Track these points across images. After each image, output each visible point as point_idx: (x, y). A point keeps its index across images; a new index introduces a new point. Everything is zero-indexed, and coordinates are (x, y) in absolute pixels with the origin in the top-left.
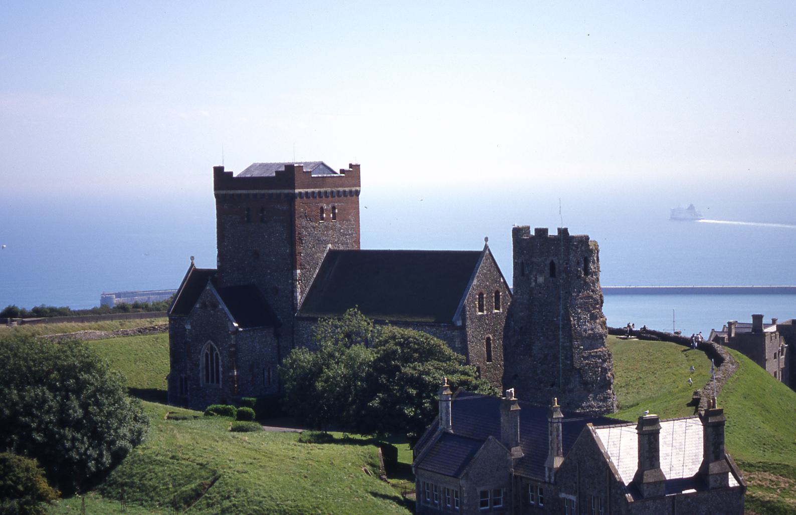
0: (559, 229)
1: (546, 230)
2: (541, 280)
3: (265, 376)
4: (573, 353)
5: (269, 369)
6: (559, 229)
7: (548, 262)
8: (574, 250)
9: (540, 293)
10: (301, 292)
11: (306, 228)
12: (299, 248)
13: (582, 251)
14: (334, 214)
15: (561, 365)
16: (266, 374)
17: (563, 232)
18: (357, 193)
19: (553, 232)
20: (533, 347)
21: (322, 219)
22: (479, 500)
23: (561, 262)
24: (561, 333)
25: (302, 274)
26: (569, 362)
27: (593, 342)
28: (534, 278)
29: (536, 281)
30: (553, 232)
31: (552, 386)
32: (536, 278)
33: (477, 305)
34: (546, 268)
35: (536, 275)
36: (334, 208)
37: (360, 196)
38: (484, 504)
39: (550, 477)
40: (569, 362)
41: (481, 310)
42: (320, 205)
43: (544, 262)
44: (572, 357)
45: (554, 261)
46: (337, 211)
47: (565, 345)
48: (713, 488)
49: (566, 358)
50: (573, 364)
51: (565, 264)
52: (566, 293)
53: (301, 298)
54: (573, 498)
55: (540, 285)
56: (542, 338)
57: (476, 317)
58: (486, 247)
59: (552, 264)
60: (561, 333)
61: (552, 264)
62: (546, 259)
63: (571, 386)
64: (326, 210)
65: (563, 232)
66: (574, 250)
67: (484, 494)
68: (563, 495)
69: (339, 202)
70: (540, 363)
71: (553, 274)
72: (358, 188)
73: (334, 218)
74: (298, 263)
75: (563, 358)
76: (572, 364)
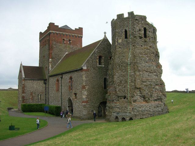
0: (129, 13)
1: (123, 14)
2: (120, 41)
4: (135, 78)
6: (129, 13)
7: (124, 30)
9: (120, 48)
13: (142, 24)
15: (129, 86)
16: (39, 96)
17: (131, 14)
18: (82, 37)
21: (64, 43)
23: (130, 30)
24: (129, 67)
25: (52, 61)
26: (133, 84)
27: (150, 74)
31: (124, 98)
32: (118, 40)
34: (123, 34)
36: (70, 40)
40: (133, 84)
41: (100, 64)
42: (64, 38)
44: (135, 80)
46: (71, 41)
49: (132, 82)
52: (133, 46)
58: (105, 36)
59: (126, 31)
60: (129, 67)
61: (126, 31)
62: (122, 30)
63: (135, 99)
64: (66, 40)
65: (131, 14)
71: (126, 37)
73: (70, 43)
75: (130, 82)
76: (135, 85)
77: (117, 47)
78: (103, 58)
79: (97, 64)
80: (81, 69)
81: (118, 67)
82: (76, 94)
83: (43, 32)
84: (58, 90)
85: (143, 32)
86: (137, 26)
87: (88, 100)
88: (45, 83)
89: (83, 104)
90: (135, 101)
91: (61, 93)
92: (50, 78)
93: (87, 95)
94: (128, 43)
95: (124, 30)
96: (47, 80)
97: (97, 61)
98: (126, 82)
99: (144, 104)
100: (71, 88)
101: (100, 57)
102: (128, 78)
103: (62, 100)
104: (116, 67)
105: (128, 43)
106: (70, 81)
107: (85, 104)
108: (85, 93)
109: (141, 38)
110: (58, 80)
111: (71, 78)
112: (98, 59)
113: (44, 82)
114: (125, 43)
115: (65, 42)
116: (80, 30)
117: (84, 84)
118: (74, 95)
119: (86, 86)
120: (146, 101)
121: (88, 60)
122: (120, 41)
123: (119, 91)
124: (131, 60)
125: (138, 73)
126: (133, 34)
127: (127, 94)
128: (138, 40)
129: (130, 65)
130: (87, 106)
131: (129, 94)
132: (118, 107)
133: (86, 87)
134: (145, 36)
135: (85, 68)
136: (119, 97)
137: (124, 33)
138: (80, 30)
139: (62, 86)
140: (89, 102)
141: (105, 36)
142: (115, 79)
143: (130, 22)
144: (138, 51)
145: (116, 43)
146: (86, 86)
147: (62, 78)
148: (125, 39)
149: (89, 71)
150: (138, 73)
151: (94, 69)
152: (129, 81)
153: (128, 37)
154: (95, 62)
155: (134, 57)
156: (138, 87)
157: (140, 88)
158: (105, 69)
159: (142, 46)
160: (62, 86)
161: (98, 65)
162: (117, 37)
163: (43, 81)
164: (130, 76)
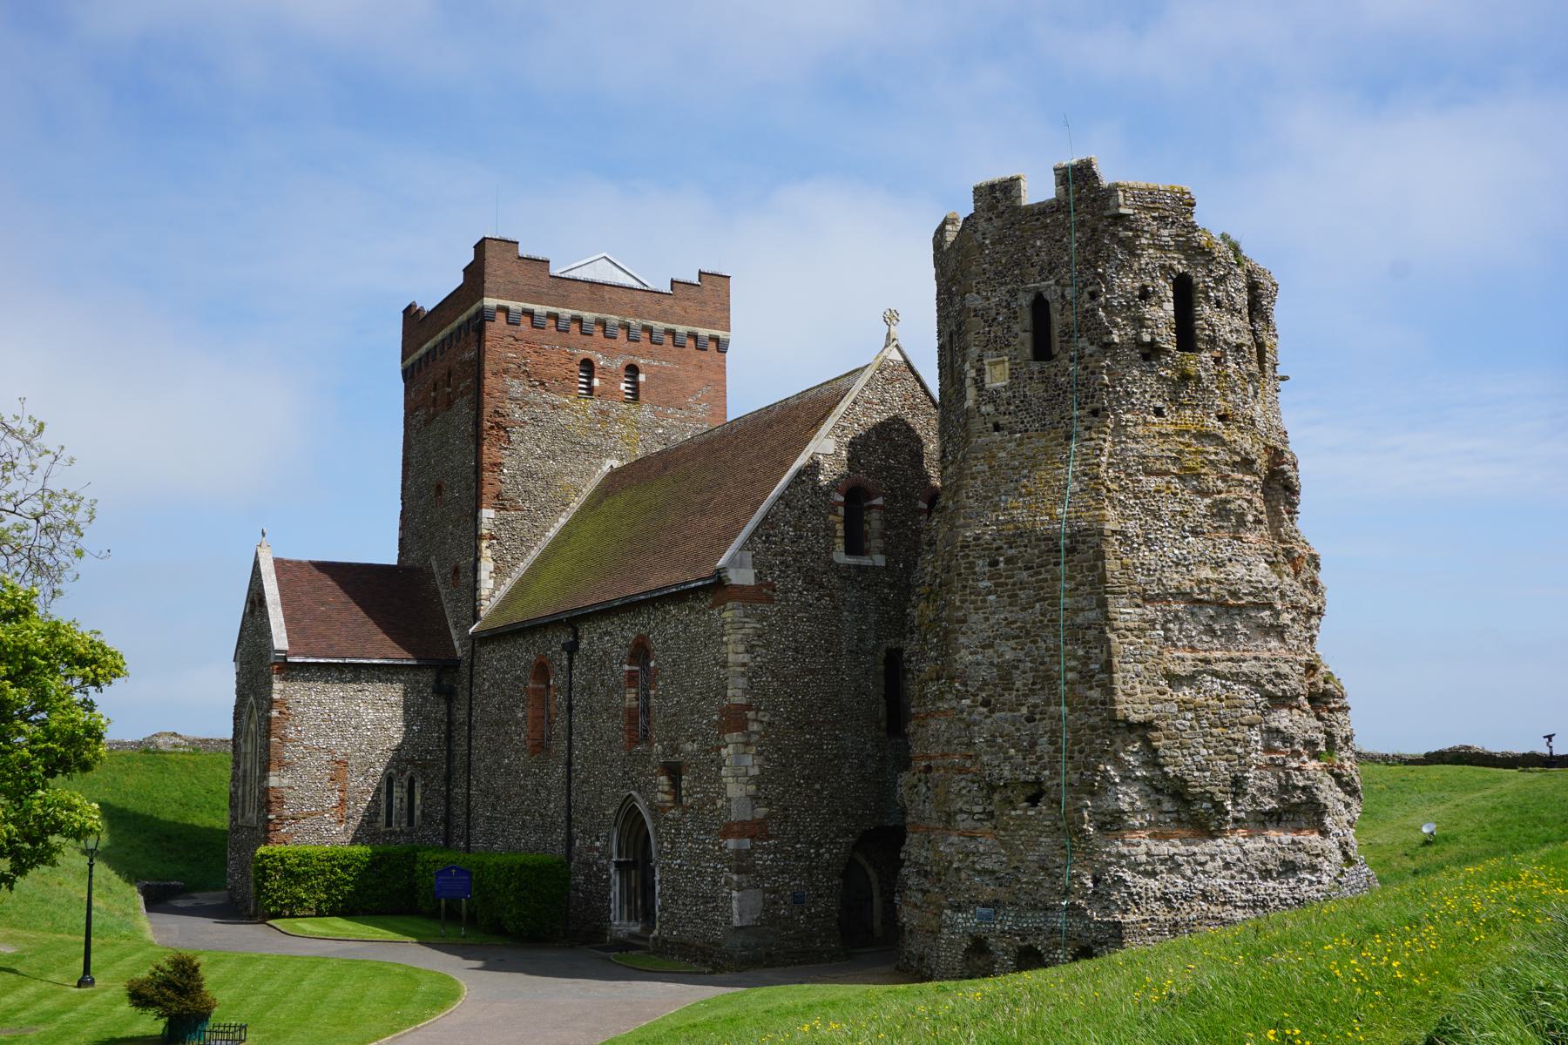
2: (997, 378)
3: (396, 802)
5: (412, 781)
7: (1025, 300)
8: (1122, 242)
9: (997, 427)
10: (497, 570)
11: (523, 403)
12: (490, 453)
14: (636, 383)
15: (1064, 709)
18: (721, 346)
20: (962, 639)
23: (1070, 293)
28: (973, 373)
29: (979, 383)
31: (1033, 800)
32: (980, 371)
33: (840, 527)
34: (1016, 328)
35: (980, 359)
40: (1095, 694)
41: (855, 545)
42: (583, 354)
43: (1008, 306)
44: (1108, 667)
45: (1047, 296)
46: (642, 378)
47: (1079, 620)
49: (1086, 677)
50: (1113, 702)
51: (1086, 296)
52: (1095, 413)
53: (496, 588)
55: (993, 398)
56: (992, 597)
57: (837, 568)
59: (1040, 306)
61: (1040, 306)
62: (1013, 293)
66: (1122, 242)
69: (652, 355)
70: (986, 703)
71: (1042, 351)
72: (720, 334)
74: (488, 491)
75: (1070, 675)
77: (977, 424)
78: (879, 501)
79: (829, 550)
80: (717, 587)
81: (981, 566)
82: (674, 771)
84: (540, 747)
85: (1169, 307)
86: (1121, 267)
87: (769, 816)
89: (731, 844)
91: (569, 764)
92: (485, 652)
93: (758, 781)
94: (1056, 396)
95: (1030, 297)
96: (464, 669)
97: (830, 529)
98: (1046, 680)
100: (638, 724)
102: (1058, 648)
103: (569, 818)
104: (972, 565)
106: (632, 677)
107: (747, 844)
108: (748, 760)
109: (1151, 352)
110: (542, 671)
111: (640, 651)
112: (841, 510)
113: (438, 681)
114: (1035, 390)
115: (596, 382)
117: (736, 695)
118: (663, 779)
119: (749, 707)
121: (765, 519)
123: (991, 742)
125: (1125, 613)
127: (1053, 765)
129: (1071, 551)
130: (763, 860)
131: (1063, 767)
132: (989, 864)
133: (751, 715)
135: (743, 576)
136: (993, 789)
137: (1026, 319)
139: (570, 708)
140: (773, 828)
142: (965, 656)
143: (1074, 239)
145: (971, 393)
146: (749, 707)
147: (572, 648)
148: (1035, 366)
149: (770, 600)
151: (811, 581)
153: (1056, 347)
154: (815, 531)
156: (1134, 718)
157: (1148, 725)
158: (891, 586)
159: (1158, 412)
160: (570, 708)
161: (840, 557)
162: (974, 351)
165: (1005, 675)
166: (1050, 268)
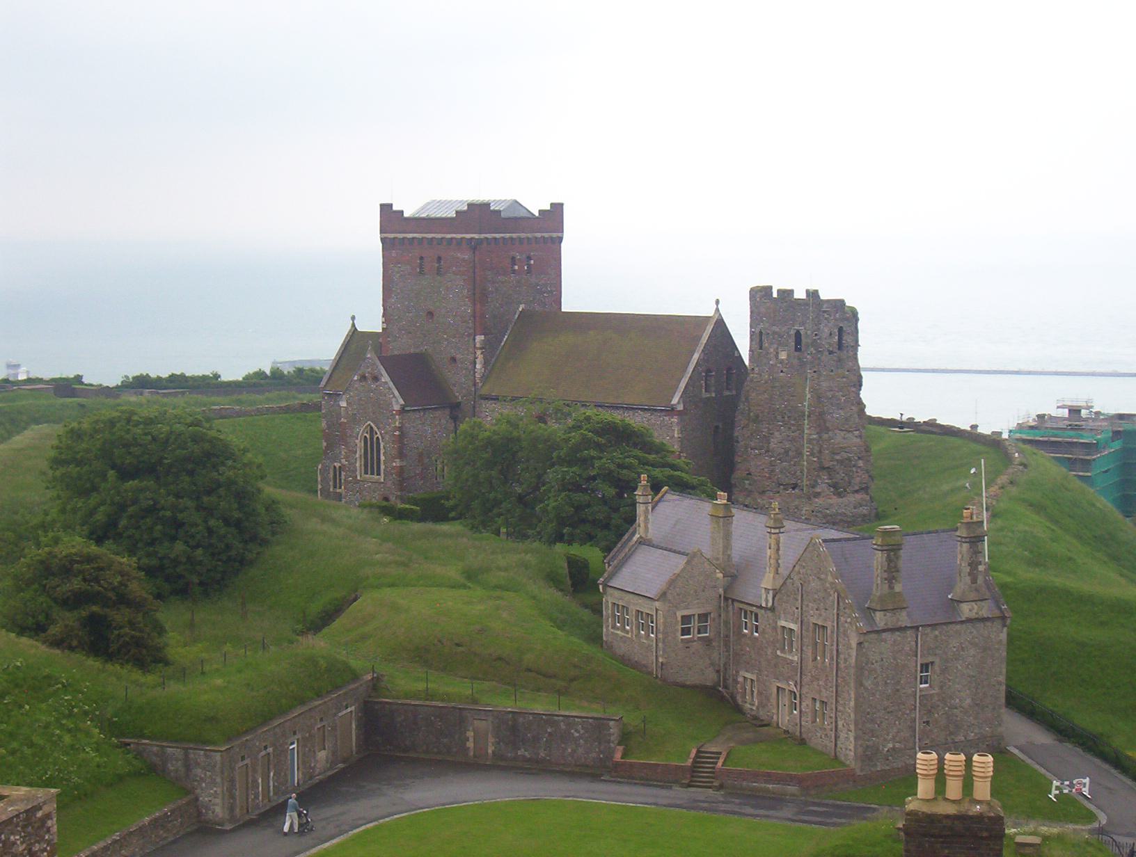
0: (807, 291)
1: (791, 292)
2: (783, 356)
6: (807, 291)
7: (793, 332)
17: (813, 294)
18: (561, 239)
19: (800, 294)
21: (514, 271)
22: (680, 627)
30: (800, 294)
36: (529, 258)
37: (563, 245)
38: (685, 631)
39: (767, 601)
44: (820, 452)
48: (969, 620)
49: (812, 454)
54: (793, 626)
55: (782, 362)
58: (717, 310)
59: (798, 334)
61: (798, 334)
63: (818, 490)
67: (686, 619)
68: (782, 623)
71: (797, 349)
81: (779, 417)
83: (406, 215)
88: (455, 419)
90: (817, 495)
94: (802, 364)
98: (800, 454)
99: (835, 500)
101: (709, 371)
105: (802, 364)
109: (831, 353)
114: (795, 361)
116: (555, 214)
120: (839, 495)
122: (783, 356)
124: (810, 405)
126: (814, 343)
128: (825, 357)
134: (840, 345)
137: (793, 338)
138: (555, 214)
141: (717, 310)
142: (772, 445)
143: (811, 316)
144: (825, 384)
150: (825, 436)
152: (806, 452)
155: (818, 397)
163: (447, 411)
164: (810, 441)
165: (787, 452)
166: (803, 324)
